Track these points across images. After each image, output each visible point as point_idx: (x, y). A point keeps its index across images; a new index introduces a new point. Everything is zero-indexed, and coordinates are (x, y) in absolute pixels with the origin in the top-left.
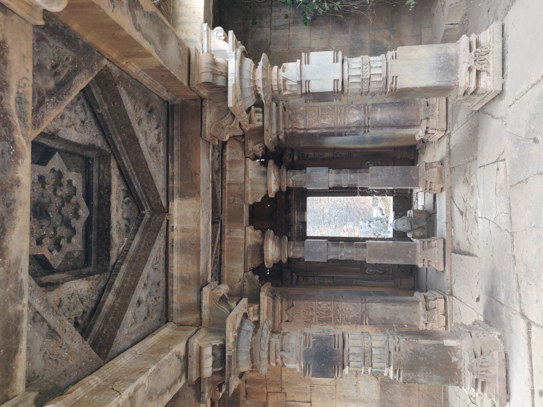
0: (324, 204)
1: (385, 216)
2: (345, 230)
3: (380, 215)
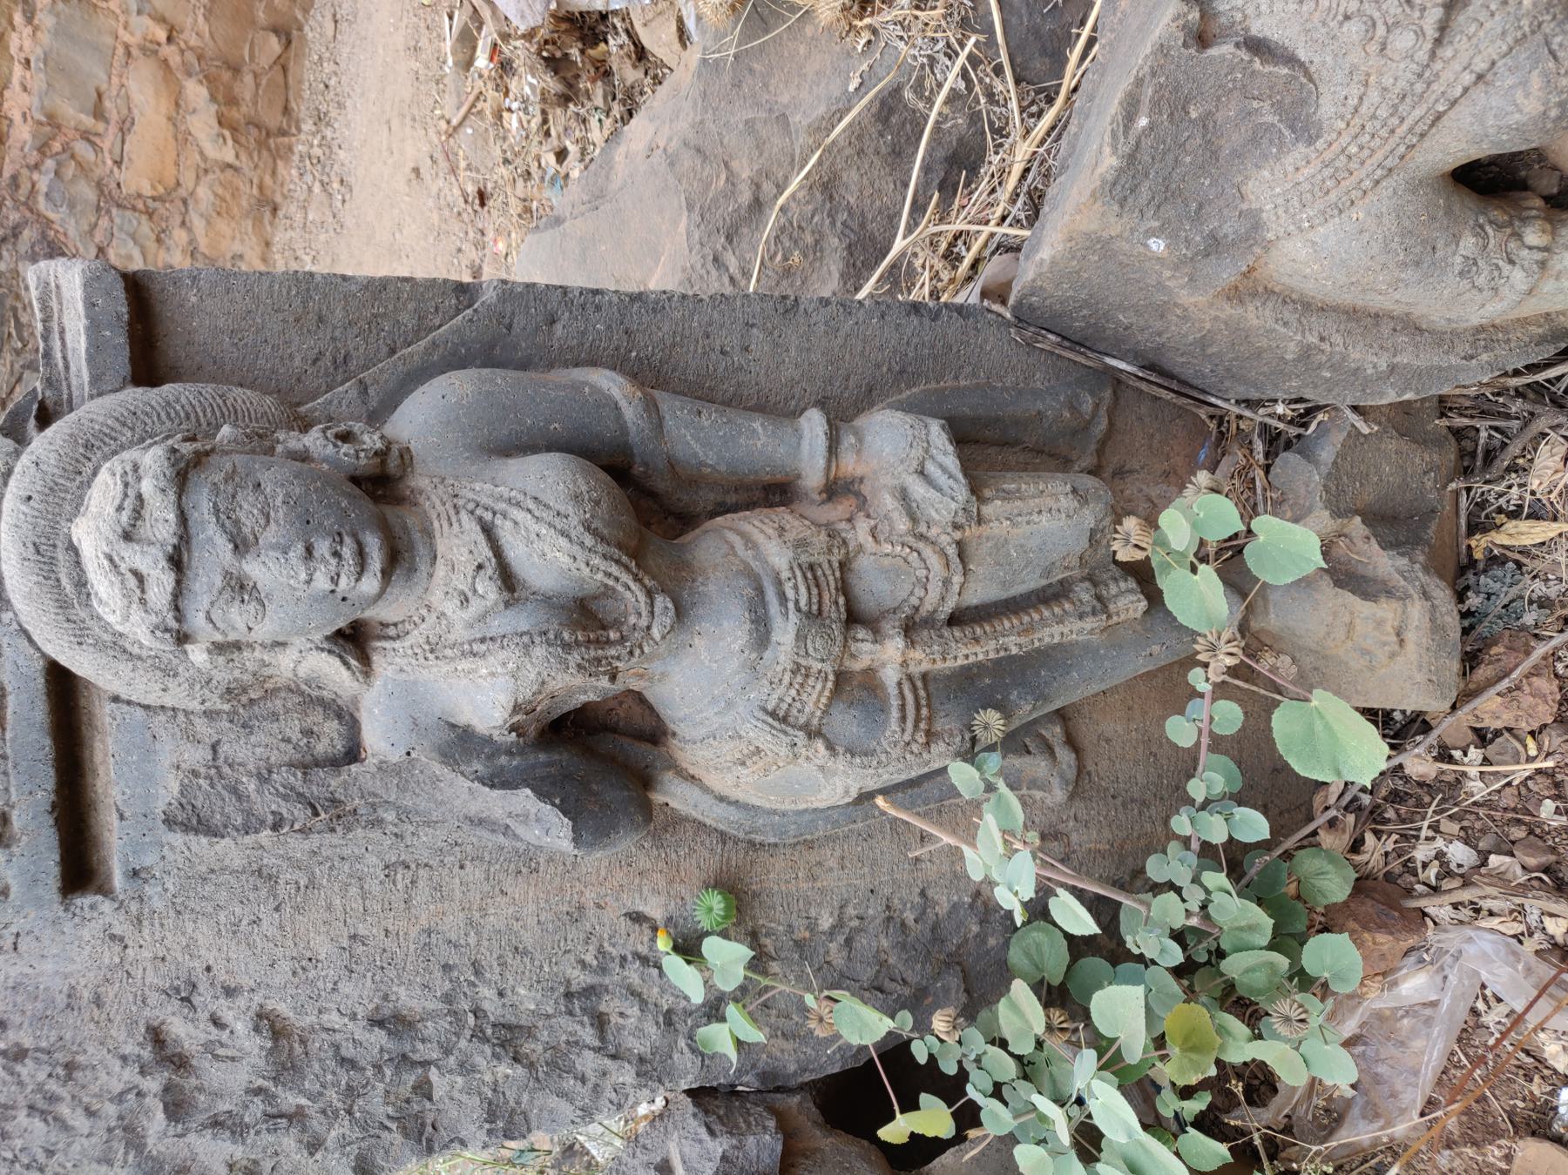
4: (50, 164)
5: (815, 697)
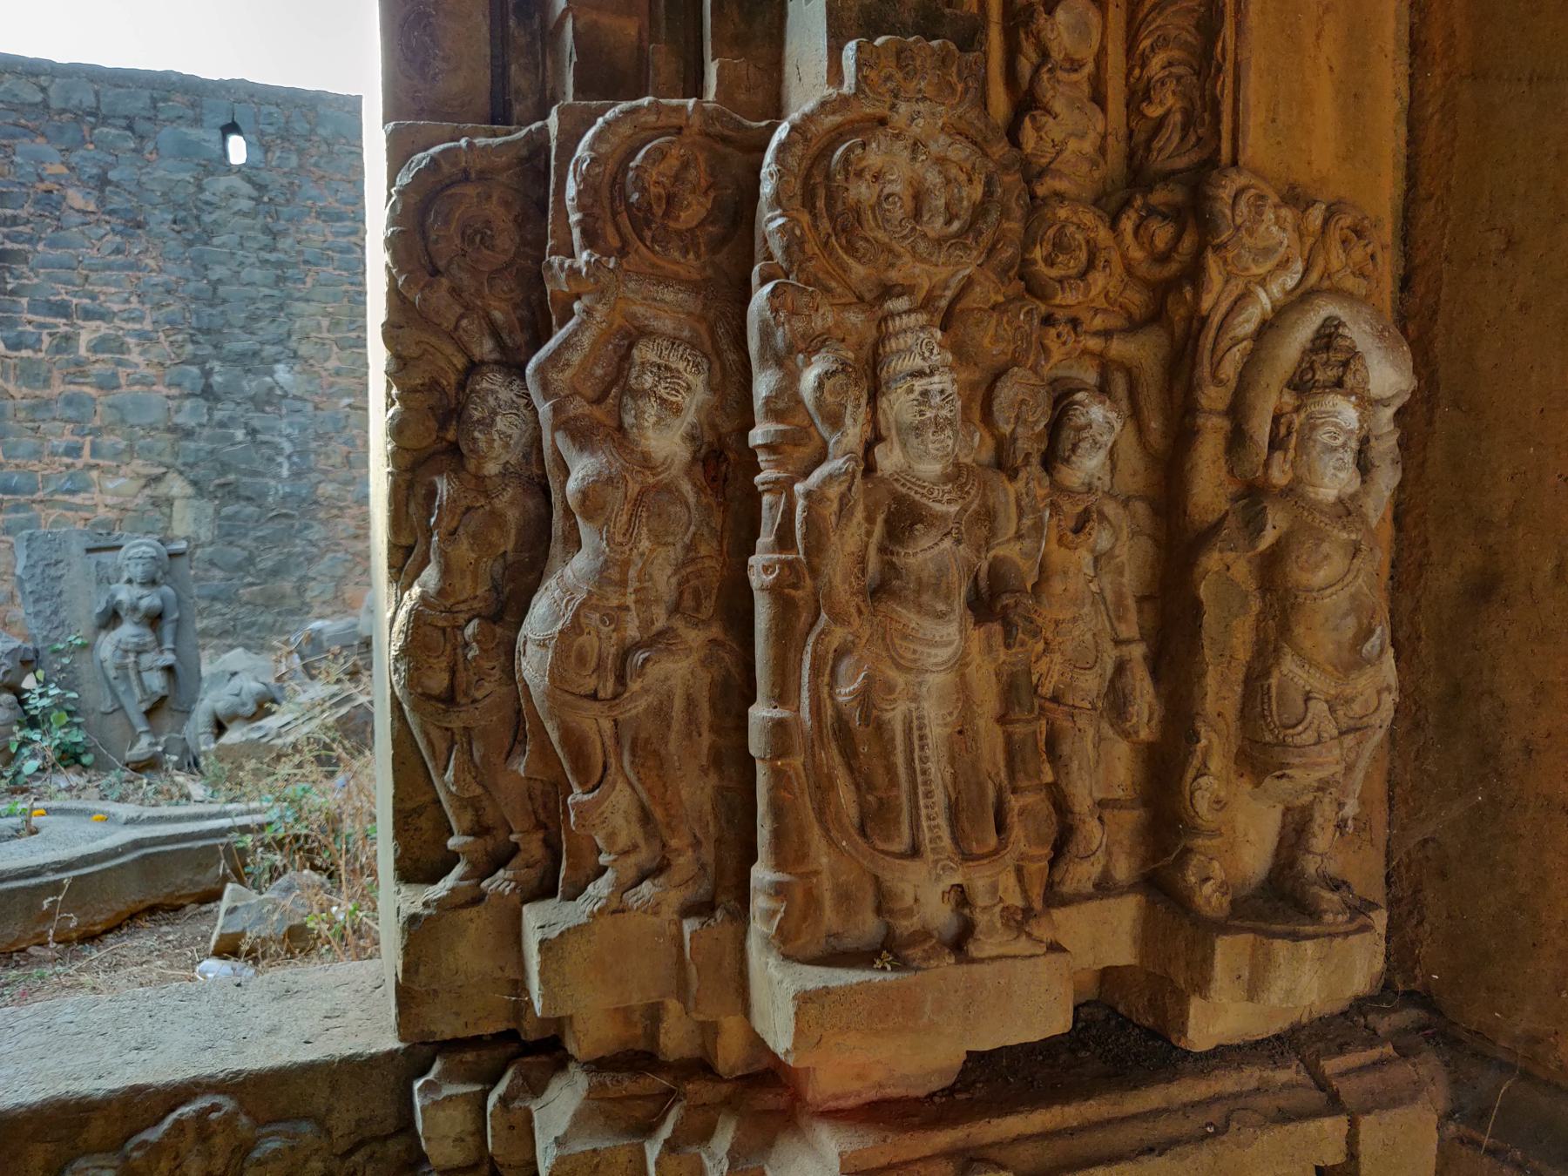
0: (332, 364)
1: (207, 745)
2: (161, 490)
3: (213, 700)
4: (349, 557)
5: (122, 646)
